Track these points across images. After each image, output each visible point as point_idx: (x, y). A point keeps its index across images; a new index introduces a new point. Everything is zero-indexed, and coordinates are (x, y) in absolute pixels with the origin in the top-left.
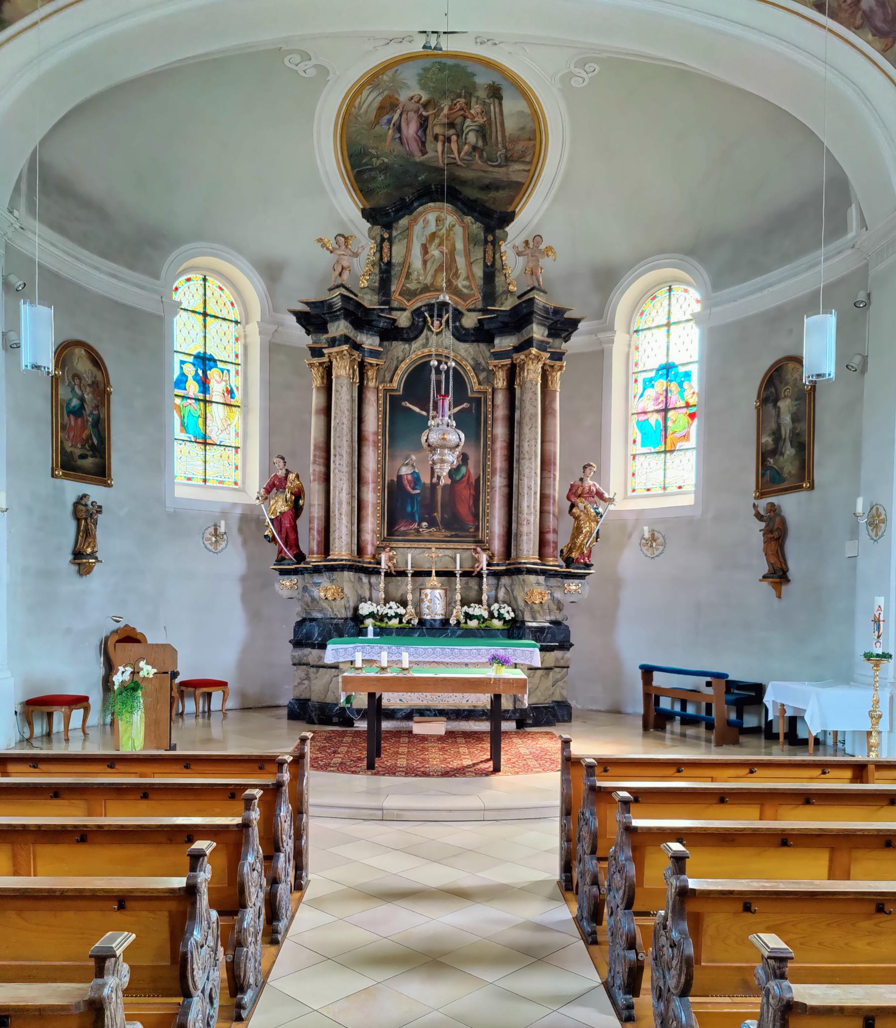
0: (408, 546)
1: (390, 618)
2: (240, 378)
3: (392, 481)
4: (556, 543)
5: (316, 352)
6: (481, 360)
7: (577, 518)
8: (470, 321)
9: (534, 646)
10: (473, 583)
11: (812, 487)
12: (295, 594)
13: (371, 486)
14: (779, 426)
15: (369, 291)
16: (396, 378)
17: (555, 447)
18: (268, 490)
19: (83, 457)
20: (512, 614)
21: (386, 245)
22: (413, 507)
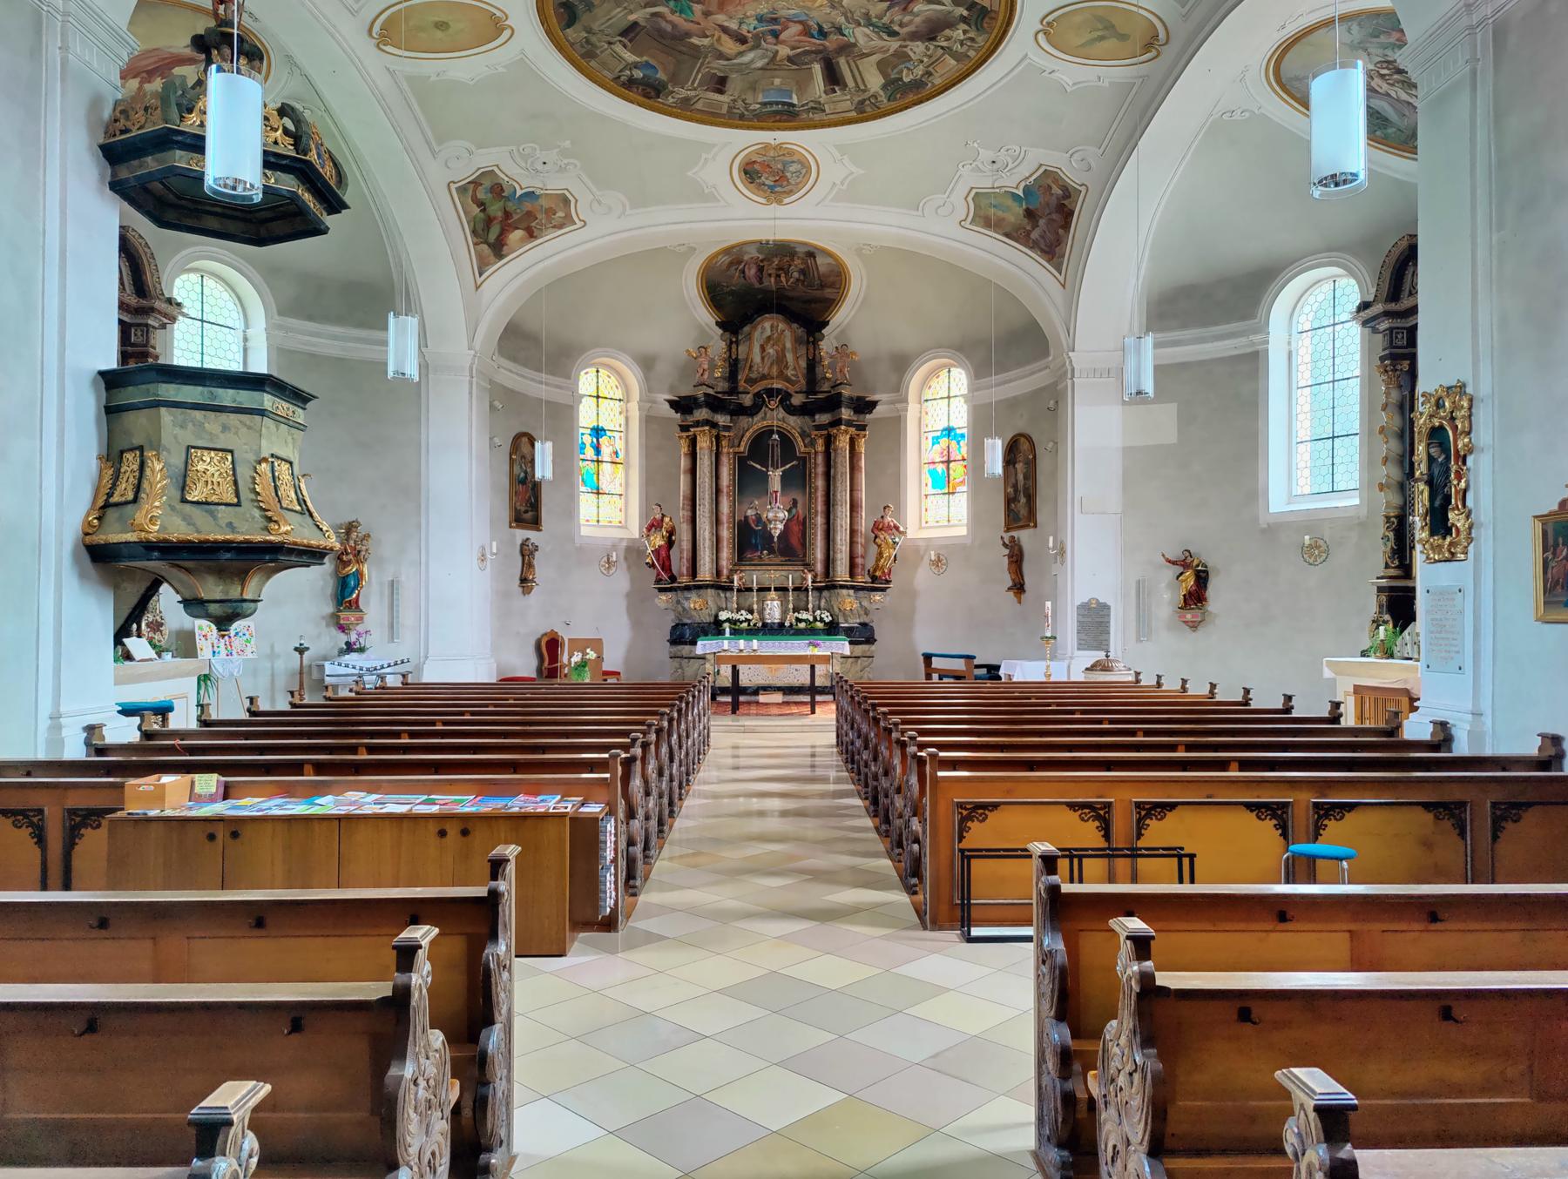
1: (741, 622)
2: (623, 442)
4: (863, 565)
5: (684, 428)
6: (806, 429)
7: (879, 546)
8: (797, 400)
9: (845, 640)
10: (802, 596)
11: (1035, 526)
12: (670, 606)
13: (725, 526)
14: (1017, 481)
16: (743, 444)
18: (649, 529)
19: (526, 512)
20: (830, 618)
21: (734, 346)
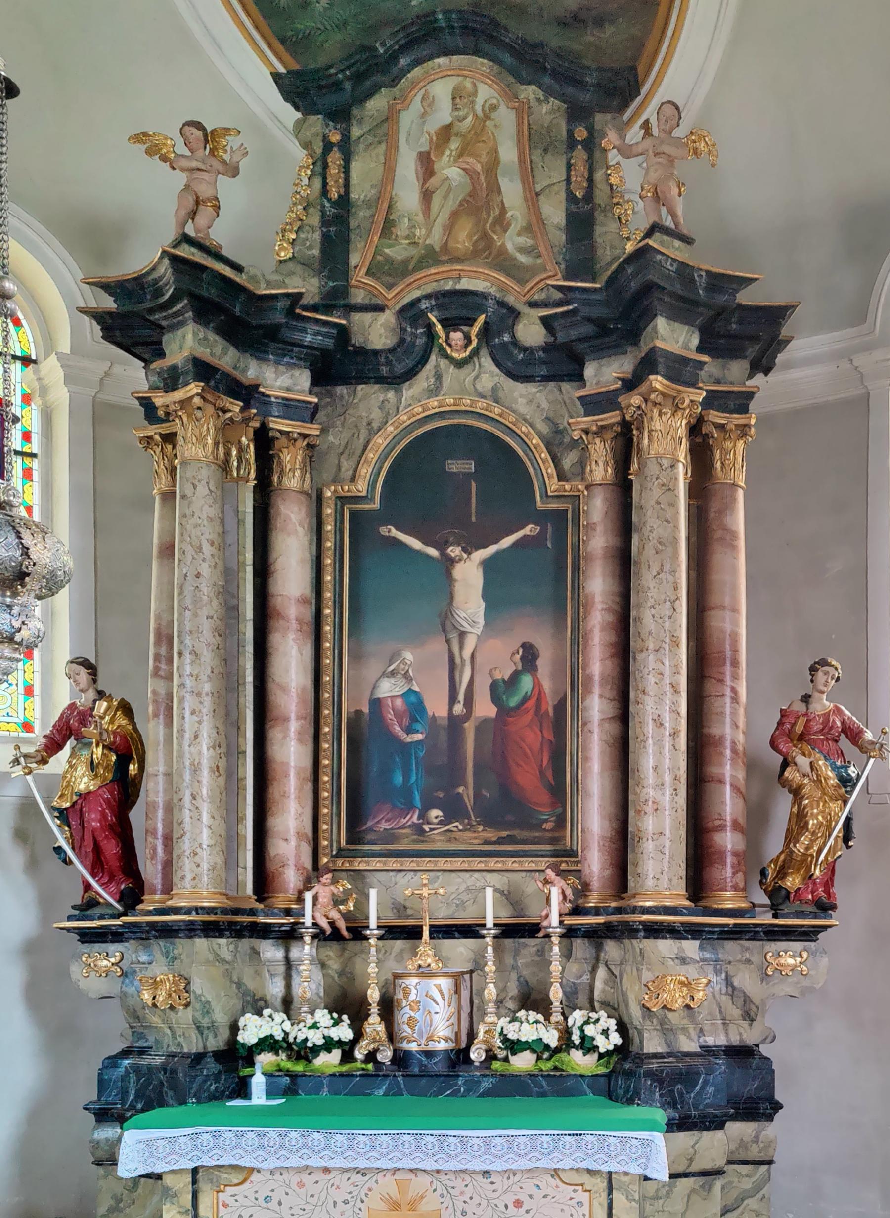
0: (396, 866)
3: (359, 713)
13: (294, 726)
15: (299, 269)
17: (736, 623)
20: (616, 1039)
21: (335, 158)
22: (406, 776)
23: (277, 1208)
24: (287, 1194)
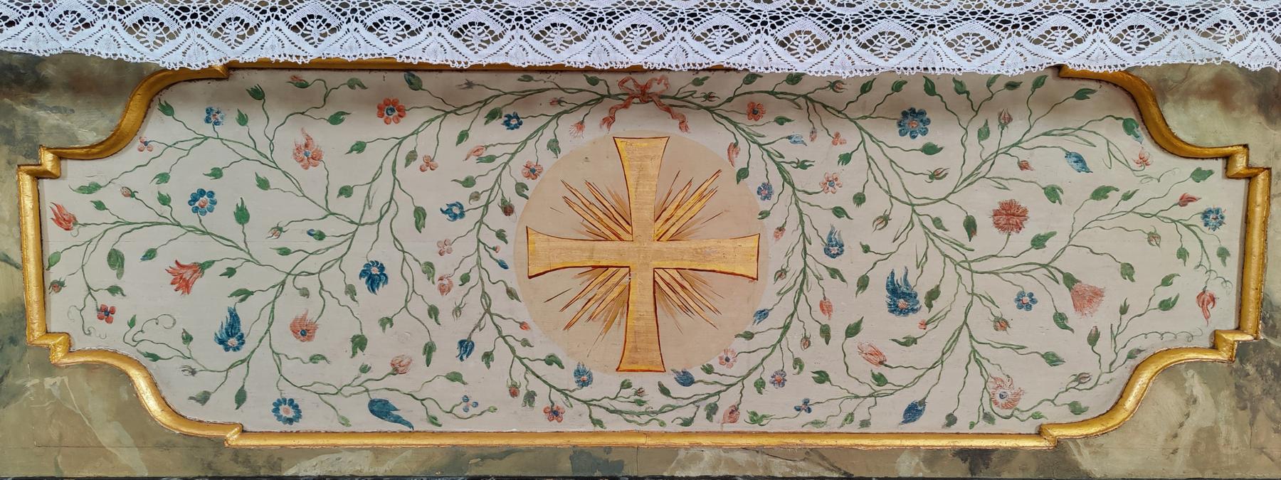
23: (230, 228)
24: (263, 184)
